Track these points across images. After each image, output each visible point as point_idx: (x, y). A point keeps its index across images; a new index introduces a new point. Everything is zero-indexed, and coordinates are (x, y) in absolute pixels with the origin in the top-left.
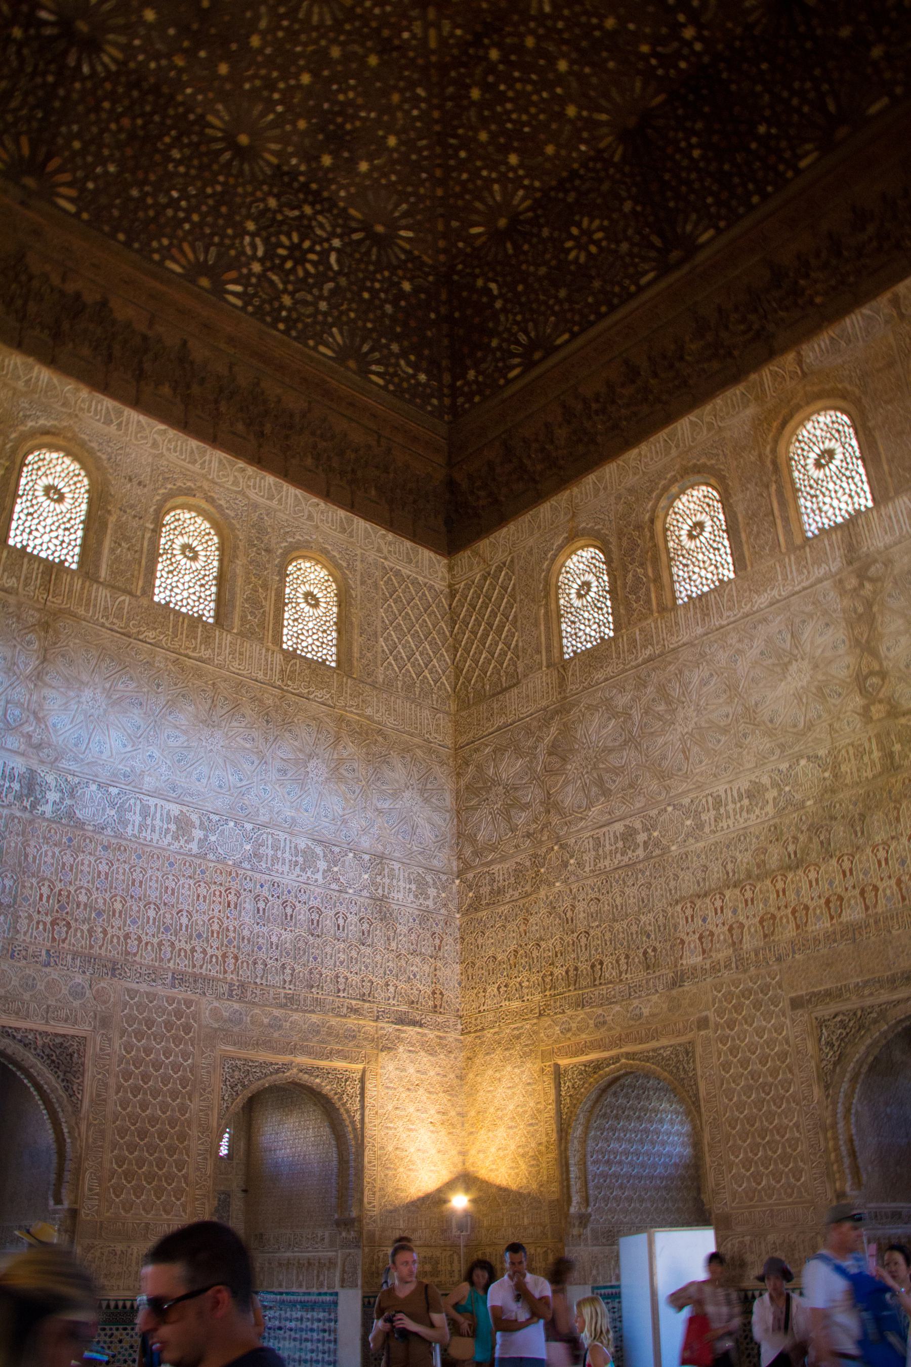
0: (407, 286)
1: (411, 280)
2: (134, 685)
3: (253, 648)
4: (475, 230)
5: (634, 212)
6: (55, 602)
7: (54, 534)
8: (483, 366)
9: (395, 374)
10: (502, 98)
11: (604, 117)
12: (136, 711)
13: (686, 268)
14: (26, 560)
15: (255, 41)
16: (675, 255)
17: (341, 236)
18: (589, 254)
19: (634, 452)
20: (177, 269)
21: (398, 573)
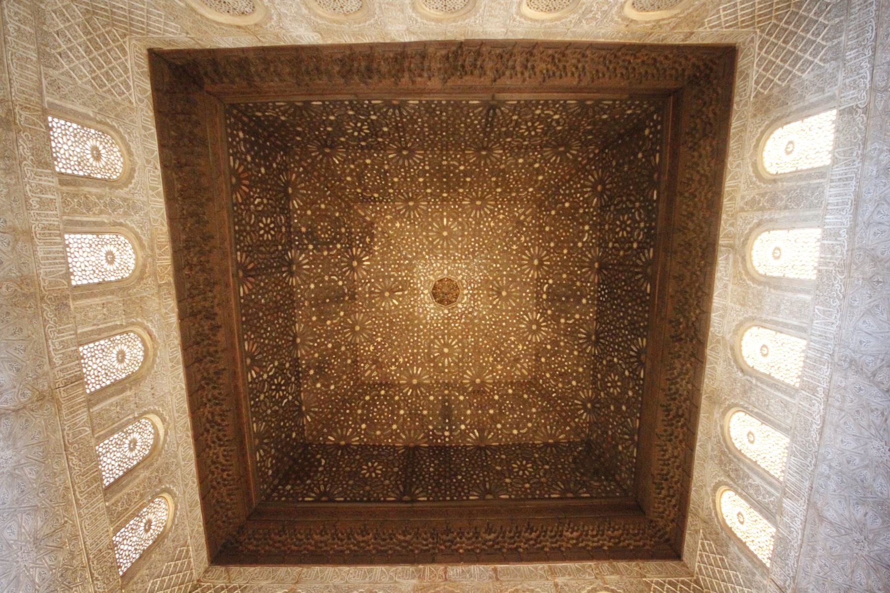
0: (294, 435)
1: (297, 434)
2: (34, 477)
3: (105, 520)
4: (330, 438)
5: (397, 472)
6: (62, 394)
7: (99, 369)
8: (297, 488)
9: (264, 461)
10: (375, 406)
11: (404, 437)
12: (15, 492)
13: (409, 505)
14: (77, 362)
15: (329, 322)
16: (406, 498)
17: (293, 398)
18: (371, 475)
19: (346, 569)
20: (246, 348)
21: (188, 551)
